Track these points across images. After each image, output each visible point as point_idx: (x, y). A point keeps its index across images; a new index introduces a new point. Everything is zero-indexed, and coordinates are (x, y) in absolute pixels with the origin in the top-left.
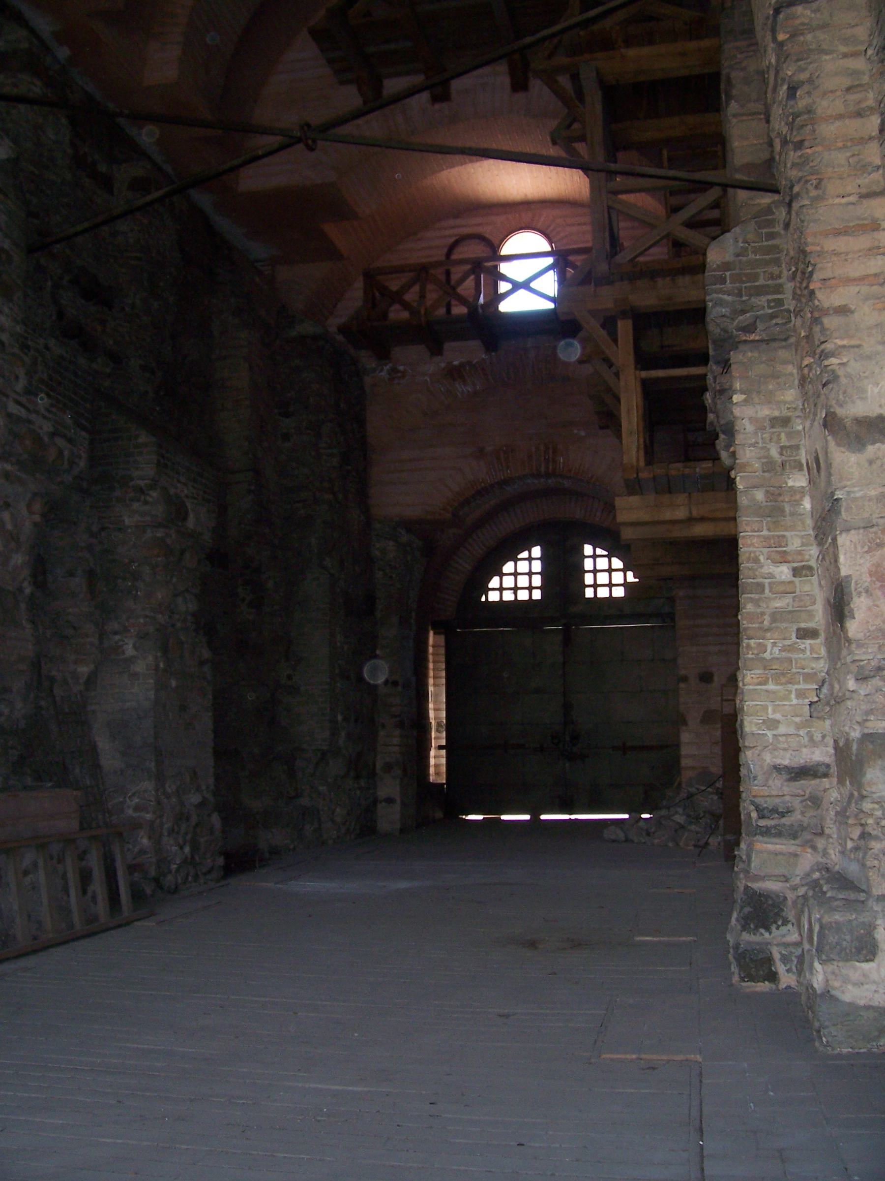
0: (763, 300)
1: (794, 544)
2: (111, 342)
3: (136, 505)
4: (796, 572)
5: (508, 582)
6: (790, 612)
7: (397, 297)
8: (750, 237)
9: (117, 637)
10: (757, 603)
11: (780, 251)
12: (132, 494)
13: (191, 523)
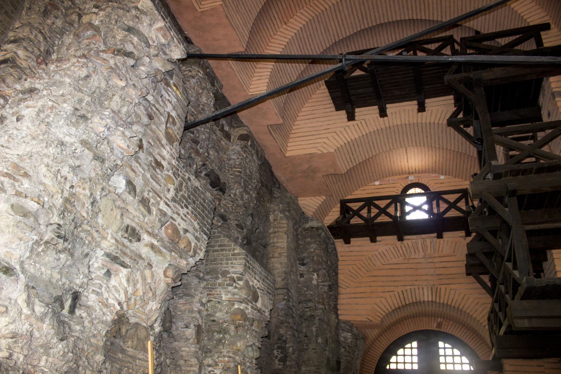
2: (222, 211)
3: (230, 288)
5: (400, 359)
7: (357, 213)
9: (210, 369)
12: (228, 282)
13: (259, 304)
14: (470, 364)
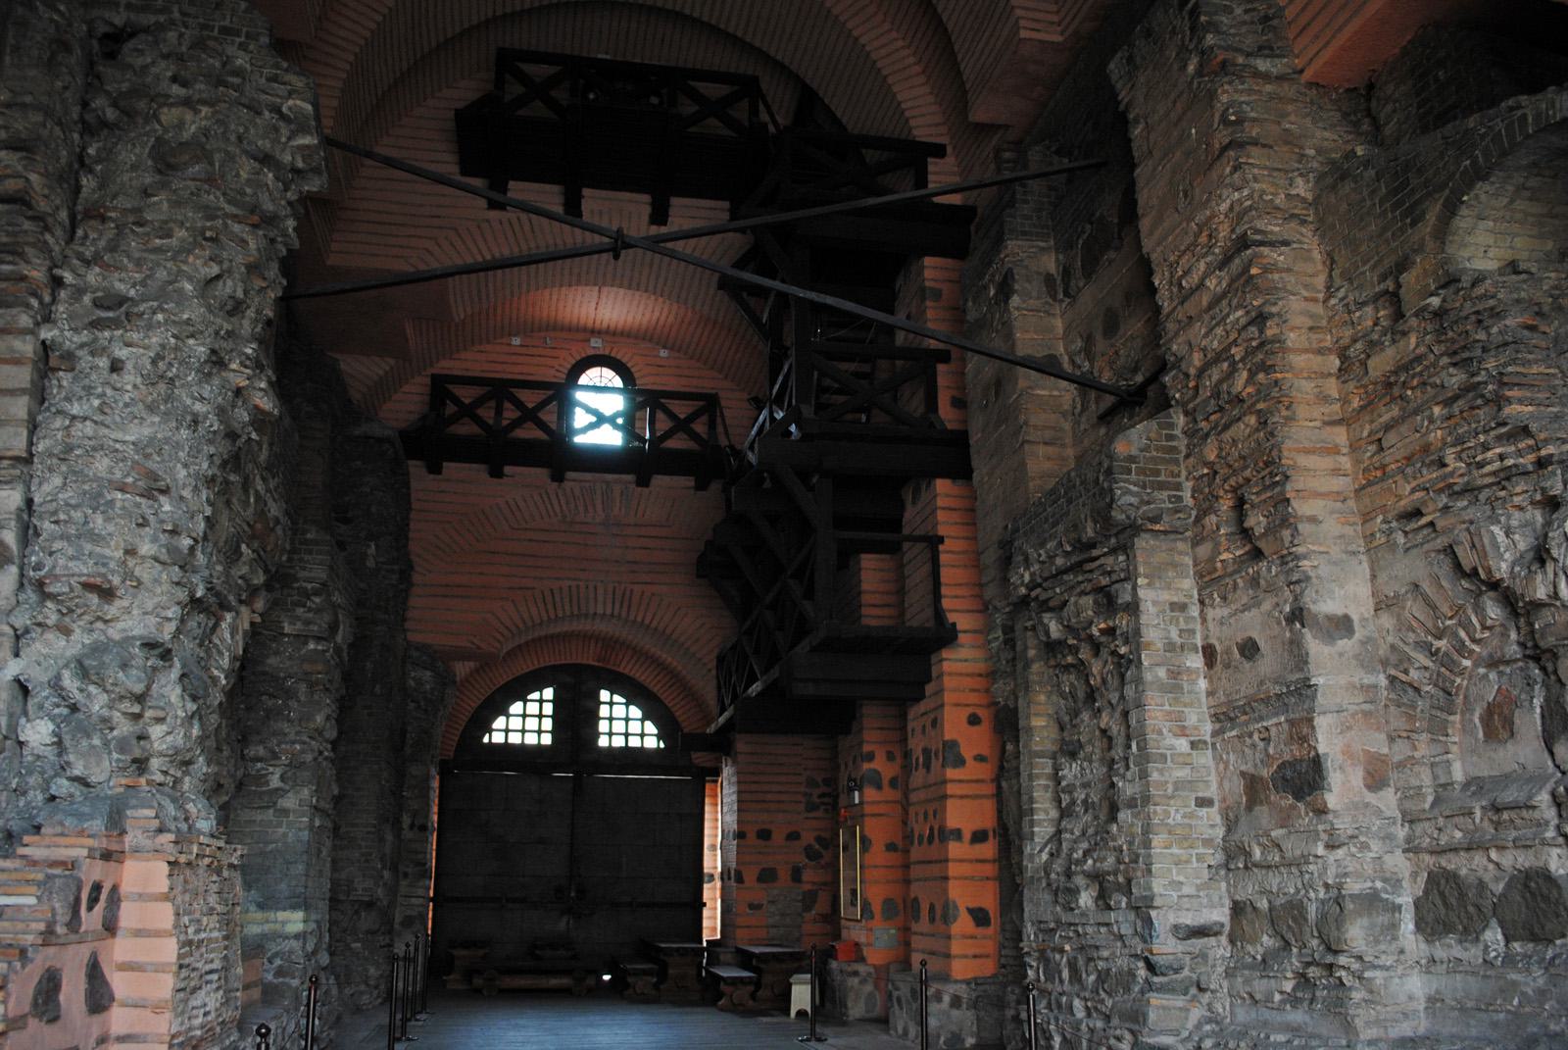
0: (1165, 494)
1: (1192, 718)
4: (1193, 745)
5: (515, 723)
6: (1190, 782)
8: (1153, 435)
10: (1161, 771)
11: (1179, 452)
14: (659, 737)
